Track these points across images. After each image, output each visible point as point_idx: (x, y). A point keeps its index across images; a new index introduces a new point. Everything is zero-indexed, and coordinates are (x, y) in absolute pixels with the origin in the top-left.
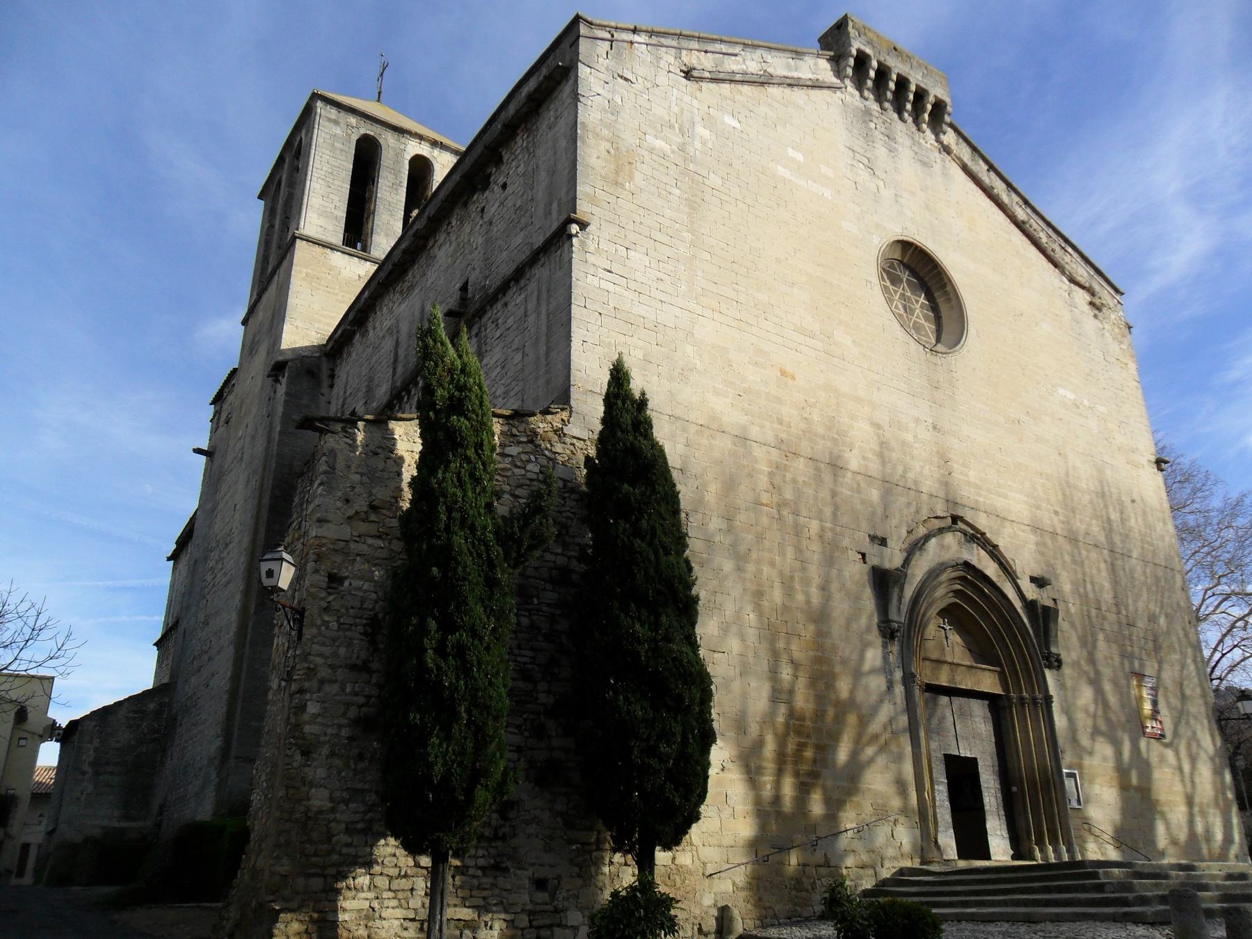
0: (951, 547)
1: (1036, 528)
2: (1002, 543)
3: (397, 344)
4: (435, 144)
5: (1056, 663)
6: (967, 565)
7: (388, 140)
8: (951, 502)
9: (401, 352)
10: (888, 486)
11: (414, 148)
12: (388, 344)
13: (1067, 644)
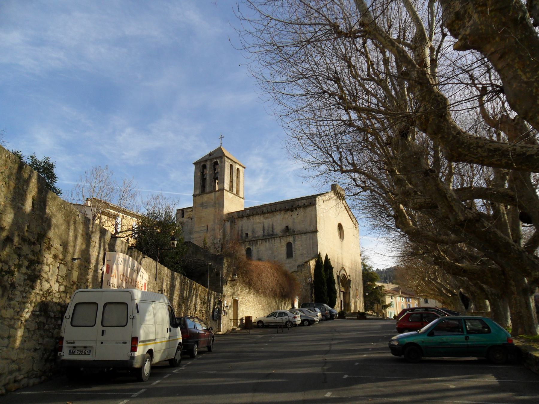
0: (343, 272)
1: (349, 268)
2: (346, 270)
3: (264, 227)
4: (240, 165)
5: (350, 287)
6: (344, 274)
7: (234, 164)
8: (343, 265)
9: (266, 229)
10: (338, 263)
11: (237, 166)
12: (261, 226)
13: (351, 284)
